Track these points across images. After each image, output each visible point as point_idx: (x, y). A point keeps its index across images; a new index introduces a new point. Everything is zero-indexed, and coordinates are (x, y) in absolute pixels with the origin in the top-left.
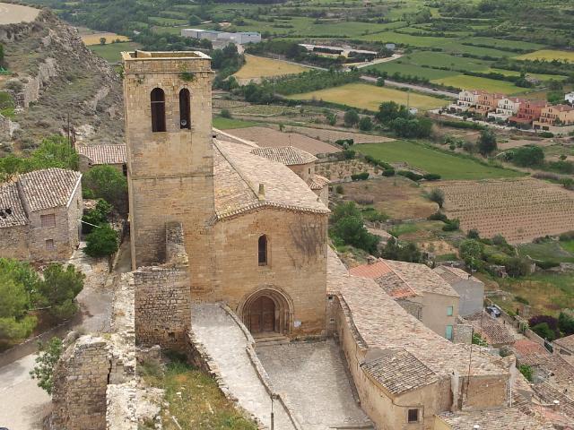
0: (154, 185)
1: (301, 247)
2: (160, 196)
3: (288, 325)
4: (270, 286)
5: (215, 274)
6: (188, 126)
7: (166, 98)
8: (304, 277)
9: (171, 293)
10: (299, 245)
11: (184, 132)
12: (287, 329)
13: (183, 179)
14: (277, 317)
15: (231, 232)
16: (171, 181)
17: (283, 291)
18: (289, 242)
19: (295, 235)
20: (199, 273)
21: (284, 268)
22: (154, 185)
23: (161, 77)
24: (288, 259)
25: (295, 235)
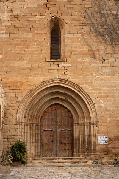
1: (102, 35)
3: (89, 142)
8: (108, 74)
10: (98, 33)
12: (88, 149)
14: (76, 134)
15: (16, 12)
17: (80, 89)
18: (87, 29)
19: (94, 21)
24: (86, 49)
25: (94, 21)
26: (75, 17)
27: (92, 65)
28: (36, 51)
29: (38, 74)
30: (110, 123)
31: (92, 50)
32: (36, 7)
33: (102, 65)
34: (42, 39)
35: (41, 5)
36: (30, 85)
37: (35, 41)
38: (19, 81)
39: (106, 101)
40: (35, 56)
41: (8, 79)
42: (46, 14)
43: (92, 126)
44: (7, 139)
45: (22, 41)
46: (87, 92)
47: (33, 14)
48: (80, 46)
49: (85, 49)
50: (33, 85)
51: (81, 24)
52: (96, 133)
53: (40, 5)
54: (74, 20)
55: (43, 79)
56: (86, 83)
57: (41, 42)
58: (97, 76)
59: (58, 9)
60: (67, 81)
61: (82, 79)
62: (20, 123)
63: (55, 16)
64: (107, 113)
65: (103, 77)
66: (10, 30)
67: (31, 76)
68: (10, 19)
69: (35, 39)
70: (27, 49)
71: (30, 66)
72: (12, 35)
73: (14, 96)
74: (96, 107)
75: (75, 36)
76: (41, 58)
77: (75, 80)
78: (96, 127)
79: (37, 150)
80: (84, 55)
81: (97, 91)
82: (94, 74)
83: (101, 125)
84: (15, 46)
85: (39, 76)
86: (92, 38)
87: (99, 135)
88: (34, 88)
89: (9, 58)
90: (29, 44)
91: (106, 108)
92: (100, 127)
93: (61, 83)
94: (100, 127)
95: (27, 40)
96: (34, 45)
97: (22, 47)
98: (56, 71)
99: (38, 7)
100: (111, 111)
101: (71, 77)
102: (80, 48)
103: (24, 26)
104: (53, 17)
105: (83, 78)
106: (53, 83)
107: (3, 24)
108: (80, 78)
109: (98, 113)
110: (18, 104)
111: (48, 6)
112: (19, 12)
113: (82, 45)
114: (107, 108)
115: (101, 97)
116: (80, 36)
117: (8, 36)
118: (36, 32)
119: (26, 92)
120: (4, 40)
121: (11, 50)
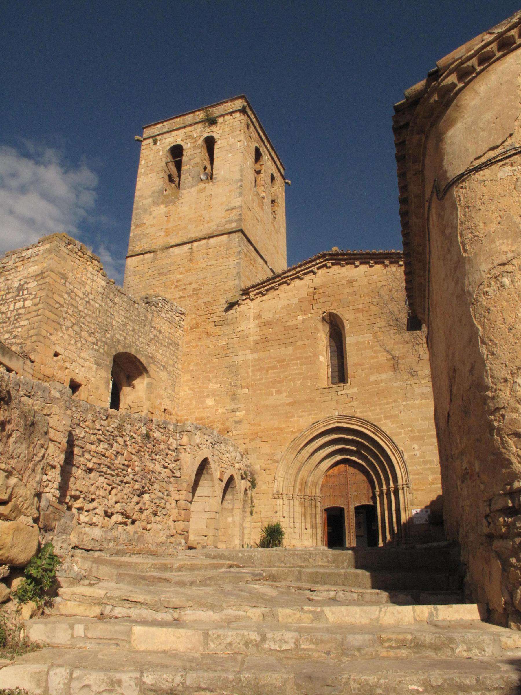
0: (154, 260)
2: (160, 274)
4: (347, 418)
5: (234, 398)
6: (210, 177)
7: (184, 153)
9: (20, 288)
11: (202, 185)
13: (195, 244)
15: (266, 316)
16: (176, 250)
17: (377, 430)
18: (381, 323)
20: (208, 396)
21: (372, 378)
22: (154, 260)
23: (181, 132)
24: (382, 358)
26: (360, 306)
27: (395, 384)
28: (300, 374)
29: (305, 412)
30: (432, 484)
31: (394, 358)
32: (297, 302)
33: (412, 382)
34: (309, 354)
35: (305, 298)
36: (293, 432)
37: (299, 359)
38: (276, 426)
39: (423, 446)
40: (300, 382)
41: (260, 425)
42: (312, 311)
43: (401, 492)
44: (261, 523)
45: (278, 361)
46: (388, 433)
47: (293, 314)
48: (373, 354)
49: (380, 359)
50: (298, 430)
51: (372, 317)
52: (409, 505)
53: (302, 298)
54: (359, 312)
55: (313, 418)
56: (386, 418)
57: (307, 358)
58: (404, 403)
59: (332, 298)
60: (353, 417)
61: (378, 410)
62: (280, 496)
63: (328, 311)
64: (425, 467)
65: (416, 402)
66: (259, 346)
67: (292, 416)
68: (258, 329)
69: (298, 355)
70: (286, 373)
71: (291, 400)
72: (263, 355)
73: (269, 451)
74: (406, 457)
75: (362, 340)
76: (309, 384)
77: (366, 414)
78: (408, 494)
79: (315, 541)
80: (378, 369)
81: (407, 429)
82: (399, 400)
83: (416, 490)
84: (267, 371)
85: (306, 414)
86: (393, 336)
87: (414, 507)
88: (300, 435)
89: (259, 391)
90: (289, 364)
91: (425, 458)
92: (415, 493)
93: (343, 422)
94: (415, 493)
95: (285, 359)
96: (296, 364)
97: (278, 370)
98: (334, 403)
99: (301, 301)
100: (433, 461)
101: (359, 410)
102: (374, 358)
103: (280, 337)
104: (325, 314)
105: (380, 409)
106: (329, 424)
107: (248, 339)
108: (374, 410)
109: (409, 468)
110: (276, 464)
111: (316, 296)
112: (271, 315)
113: (375, 352)
114: (427, 458)
115: (413, 439)
116: (371, 338)
117: (257, 357)
118: (298, 343)
119: (288, 444)
120: (251, 364)
121: (261, 379)
